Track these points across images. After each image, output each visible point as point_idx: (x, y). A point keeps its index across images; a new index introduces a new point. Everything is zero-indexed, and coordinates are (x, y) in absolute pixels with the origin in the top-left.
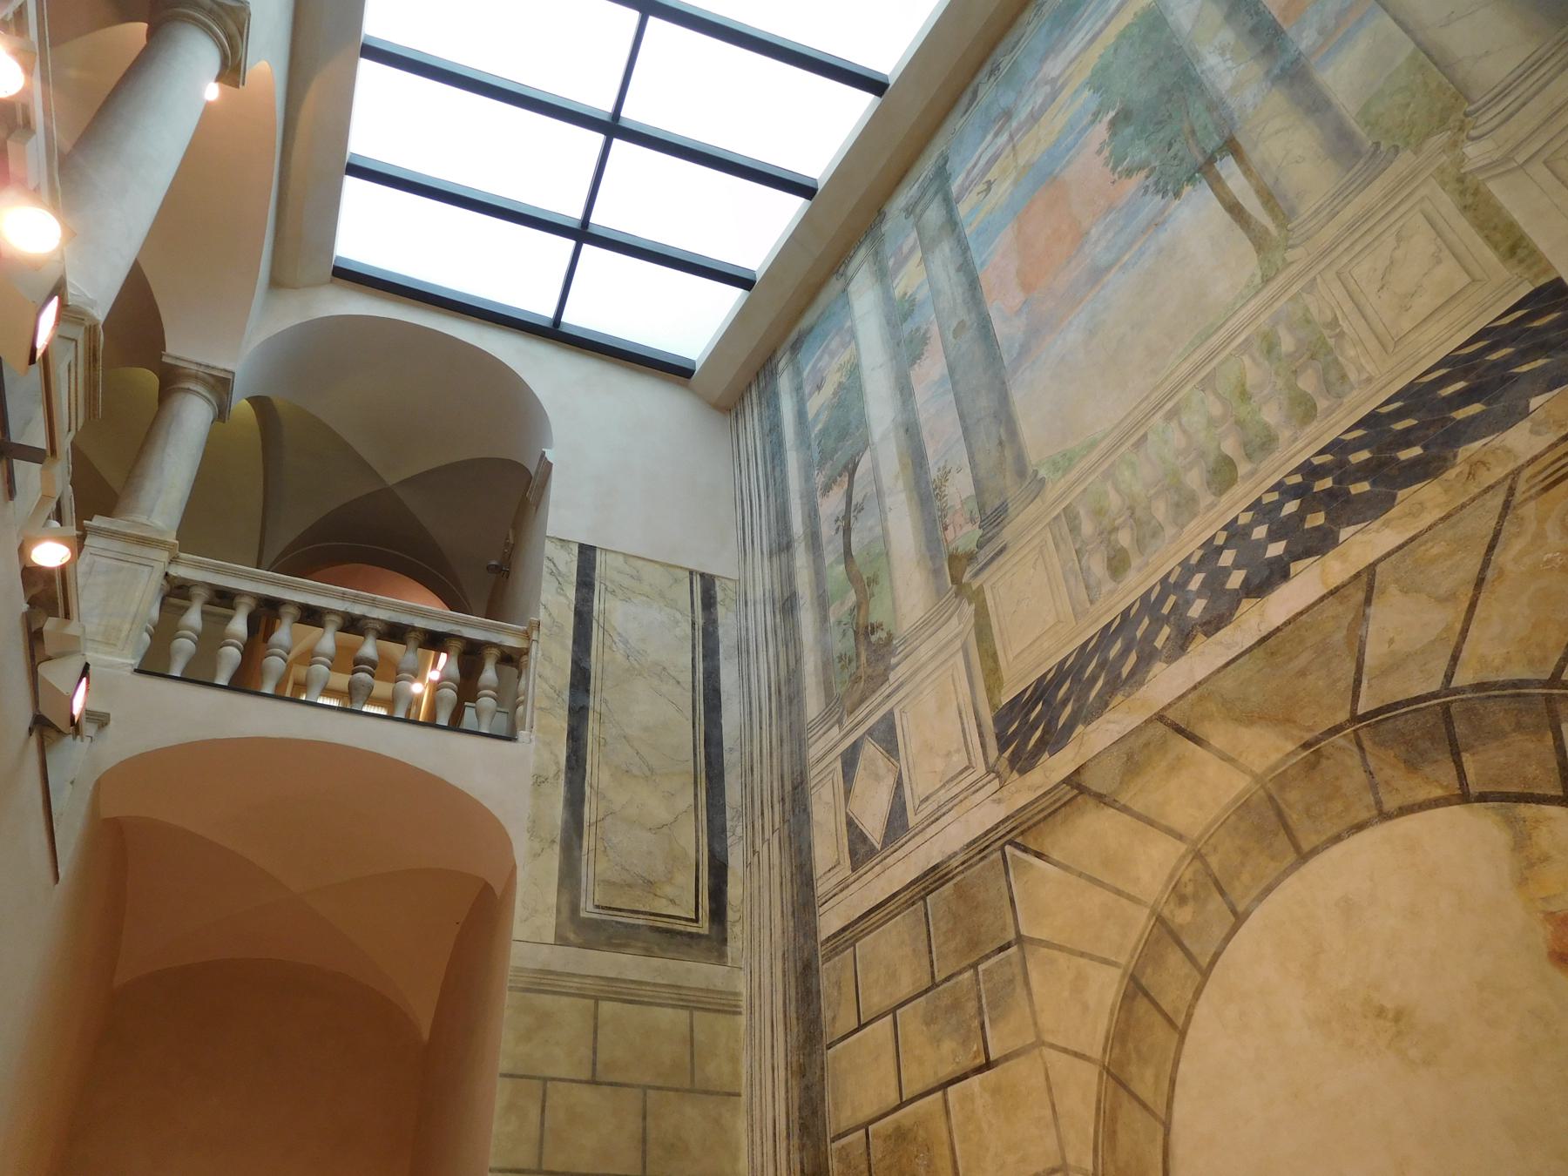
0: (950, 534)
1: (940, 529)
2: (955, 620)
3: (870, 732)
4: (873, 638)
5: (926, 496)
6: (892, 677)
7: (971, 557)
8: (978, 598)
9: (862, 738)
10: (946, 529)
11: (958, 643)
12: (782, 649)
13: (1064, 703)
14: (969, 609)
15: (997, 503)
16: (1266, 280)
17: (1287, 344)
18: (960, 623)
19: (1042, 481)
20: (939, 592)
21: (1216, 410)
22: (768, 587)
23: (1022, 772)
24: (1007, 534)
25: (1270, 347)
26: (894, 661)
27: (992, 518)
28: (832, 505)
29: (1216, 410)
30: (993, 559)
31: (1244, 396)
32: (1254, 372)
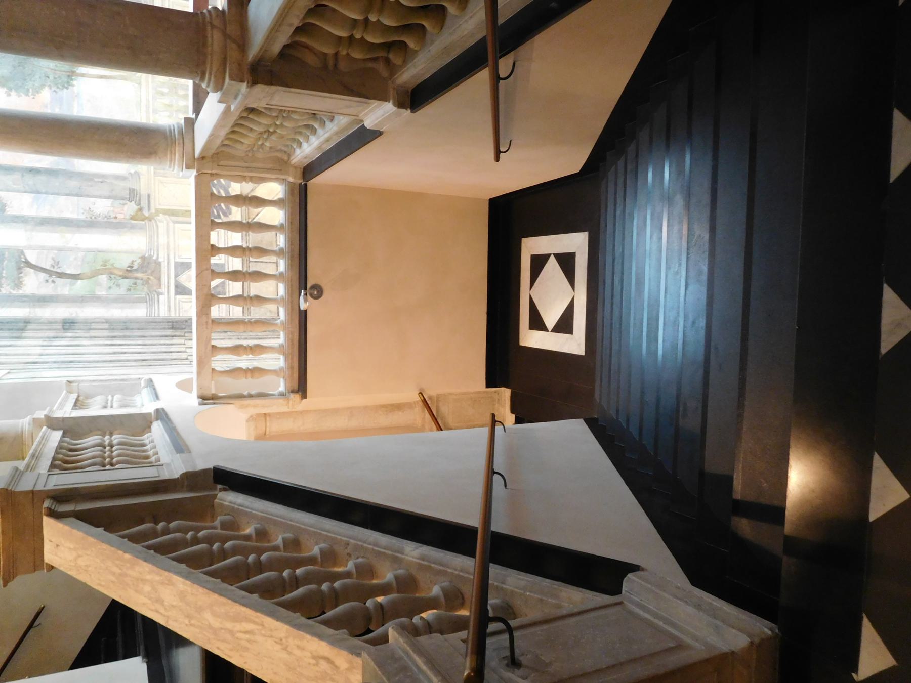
0: (120, 216)
1: (114, 221)
2: (159, 224)
3: (176, 276)
4: (135, 267)
5: (91, 224)
6: (160, 260)
7: (141, 210)
8: (158, 212)
9: (176, 281)
10: (116, 218)
11: (171, 224)
12: (92, 333)
13: (219, 192)
14: (161, 216)
15: (128, 192)
16: (140, 84)
17: (165, 90)
18: (163, 222)
19: (135, 172)
20: (142, 228)
21: (167, 114)
22: (40, 342)
23: (230, 213)
24: (144, 192)
25: (163, 94)
26: (154, 258)
27: (133, 195)
28: (33, 283)
29: (167, 114)
30: (149, 202)
31: (170, 106)
32: (166, 100)
